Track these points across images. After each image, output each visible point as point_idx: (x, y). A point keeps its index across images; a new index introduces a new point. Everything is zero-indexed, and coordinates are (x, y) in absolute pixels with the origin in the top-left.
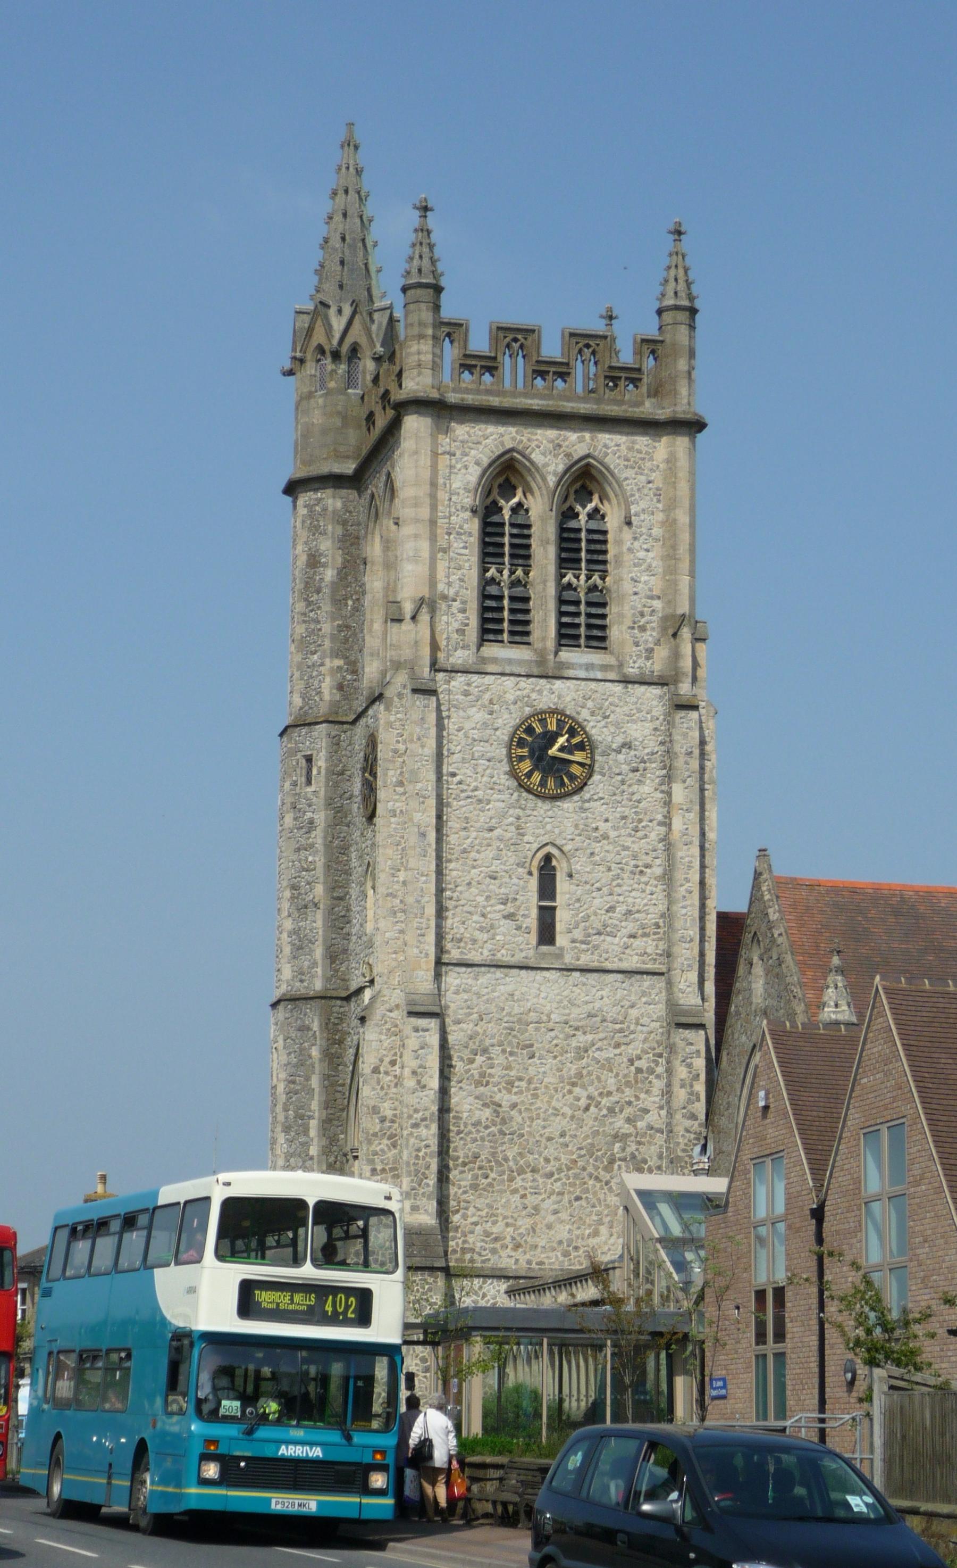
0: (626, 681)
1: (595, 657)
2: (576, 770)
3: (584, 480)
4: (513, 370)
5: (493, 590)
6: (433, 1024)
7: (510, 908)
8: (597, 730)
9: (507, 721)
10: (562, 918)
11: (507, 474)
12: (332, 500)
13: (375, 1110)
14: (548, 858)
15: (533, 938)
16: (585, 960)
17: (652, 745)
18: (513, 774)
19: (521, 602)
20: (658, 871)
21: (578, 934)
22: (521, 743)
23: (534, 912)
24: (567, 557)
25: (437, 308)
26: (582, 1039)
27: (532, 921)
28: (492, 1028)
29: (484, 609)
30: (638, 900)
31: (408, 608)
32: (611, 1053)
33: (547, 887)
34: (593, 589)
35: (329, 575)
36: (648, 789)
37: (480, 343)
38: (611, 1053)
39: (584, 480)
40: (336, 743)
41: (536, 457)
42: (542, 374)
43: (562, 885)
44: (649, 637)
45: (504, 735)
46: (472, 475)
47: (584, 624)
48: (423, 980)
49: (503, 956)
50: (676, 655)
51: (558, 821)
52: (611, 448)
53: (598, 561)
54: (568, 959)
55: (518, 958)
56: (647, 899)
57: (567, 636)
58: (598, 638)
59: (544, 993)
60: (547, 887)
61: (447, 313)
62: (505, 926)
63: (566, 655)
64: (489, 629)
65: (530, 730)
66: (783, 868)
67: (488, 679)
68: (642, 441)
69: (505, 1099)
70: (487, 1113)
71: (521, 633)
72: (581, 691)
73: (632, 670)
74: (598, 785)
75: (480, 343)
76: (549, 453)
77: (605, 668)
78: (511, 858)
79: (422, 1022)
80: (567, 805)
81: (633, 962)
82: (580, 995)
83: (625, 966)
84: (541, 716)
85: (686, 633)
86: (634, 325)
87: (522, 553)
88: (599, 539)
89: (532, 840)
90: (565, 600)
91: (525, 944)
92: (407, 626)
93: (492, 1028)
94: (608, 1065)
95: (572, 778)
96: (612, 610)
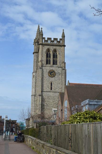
0: (59, 67)
1: (56, 65)
2: (54, 75)
3: (55, 51)
4: (49, 42)
6: (41, 96)
7: (48, 87)
9: (48, 71)
11: (48, 50)
12: (36, 54)
13: (36, 104)
14: (52, 82)
15: (50, 89)
16: (55, 91)
17: (61, 73)
19: (50, 61)
20: (61, 83)
21: (54, 89)
22: (49, 73)
23: (50, 87)
24: (54, 57)
25: (42, 36)
27: (50, 88)
28: (46, 97)
29: (47, 61)
30: (59, 86)
31: (40, 61)
32: (57, 99)
34: (56, 60)
35: (36, 60)
37: (46, 39)
38: (57, 99)
40: (36, 74)
41: (51, 49)
44: (60, 64)
45: (48, 72)
46: (46, 50)
47: (55, 63)
48: (40, 93)
49: (47, 91)
50: (63, 65)
51: (52, 79)
52: (57, 48)
53: (56, 57)
54: (53, 91)
55: (49, 91)
56: (60, 86)
57: (54, 64)
58: (57, 64)
59: (51, 94)
61: (44, 37)
62: (48, 88)
63: (54, 65)
64: (47, 63)
65: (50, 71)
66: (70, 82)
68: (60, 47)
71: (50, 64)
72: (54, 68)
73: (59, 67)
74: (56, 76)
75: (46, 39)
76: (52, 48)
77: (57, 66)
78: (48, 82)
79: (40, 96)
80: (54, 78)
81: (59, 91)
82: (54, 94)
83: (58, 92)
84: (51, 70)
85: (64, 63)
86: (59, 37)
87: (50, 57)
88: (57, 56)
89: (50, 81)
90: (54, 61)
91: (49, 90)
92: (40, 63)
93: (46, 97)
94: (57, 100)
96: (58, 61)
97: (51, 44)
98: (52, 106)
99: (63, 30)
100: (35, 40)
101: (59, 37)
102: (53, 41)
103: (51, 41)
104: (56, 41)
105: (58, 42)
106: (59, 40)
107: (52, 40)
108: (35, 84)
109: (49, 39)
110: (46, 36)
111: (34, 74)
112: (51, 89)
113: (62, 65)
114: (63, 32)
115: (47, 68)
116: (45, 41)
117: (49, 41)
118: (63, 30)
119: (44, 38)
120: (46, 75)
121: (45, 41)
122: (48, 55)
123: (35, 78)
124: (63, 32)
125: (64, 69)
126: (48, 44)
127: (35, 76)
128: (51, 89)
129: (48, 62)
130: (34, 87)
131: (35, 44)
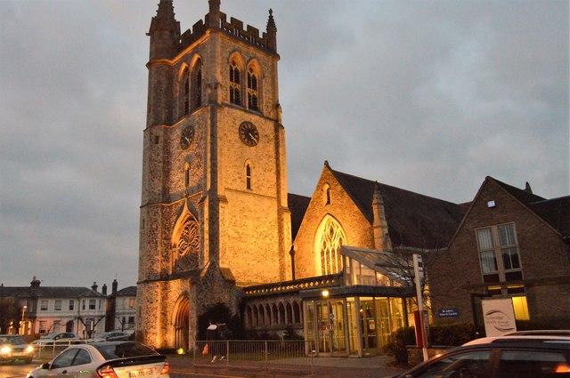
8: (260, 131)
9: (238, 123)
10: (253, 181)
18: (240, 138)
24: (249, 87)
26: (258, 216)
33: (249, 174)
36: (271, 147)
40: (166, 131)
43: (253, 172)
53: (255, 88)
60: (249, 174)
67: (235, 111)
69: (239, 230)
70: (236, 235)
74: (260, 145)
91: (245, 189)
98: (253, 240)
99: (271, 11)
100: (156, 22)
101: (262, 29)
106: (261, 36)
108: (161, 165)
109: (237, 24)
111: (159, 131)
112: (249, 187)
113: (272, 114)
114: (271, 17)
115: (239, 116)
118: (271, 11)
119: (224, 16)
120: (234, 136)
122: (235, 76)
123: (160, 145)
124: (271, 17)
125: (278, 126)
127: (161, 139)
128: (249, 187)
129: (236, 99)
130: (160, 174)
131: (157, 33)
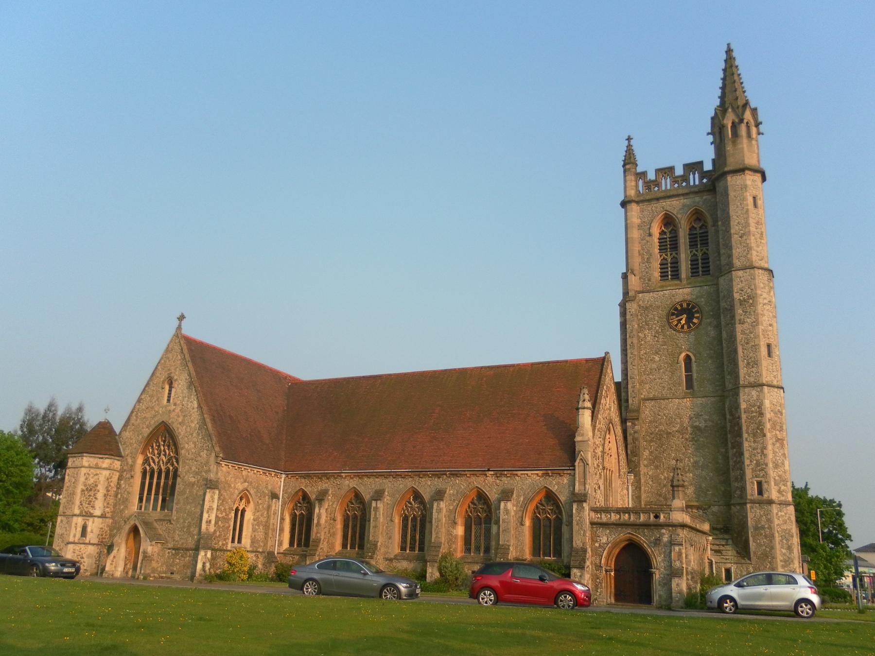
2: (695, 321)
5: (665, 262)
19: (675, 263)
24: (693, 244)
39: (697, 216)
42: (676, 182)
53: (705, 243)
57: (694, 272)
61: (639, 169)
64: (664, 275)
71: (676, 276)
75: (651, 176)
95: (694, 324)
97: (675, 193)
102: (685, 178)
103: (675, 180)
104: (697, 175)
105: (704, 174)
107: (679, 171)
109: (668, 171)
110: (648, 164)
116: (648, 184)
117: (663, 181)
119: (644, 174)
121: (648, 184)
126: (662, 195)
129: (670, 271)
